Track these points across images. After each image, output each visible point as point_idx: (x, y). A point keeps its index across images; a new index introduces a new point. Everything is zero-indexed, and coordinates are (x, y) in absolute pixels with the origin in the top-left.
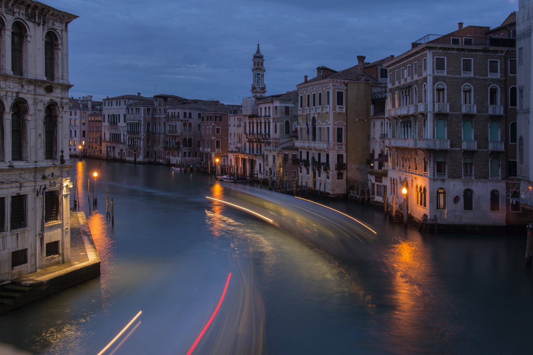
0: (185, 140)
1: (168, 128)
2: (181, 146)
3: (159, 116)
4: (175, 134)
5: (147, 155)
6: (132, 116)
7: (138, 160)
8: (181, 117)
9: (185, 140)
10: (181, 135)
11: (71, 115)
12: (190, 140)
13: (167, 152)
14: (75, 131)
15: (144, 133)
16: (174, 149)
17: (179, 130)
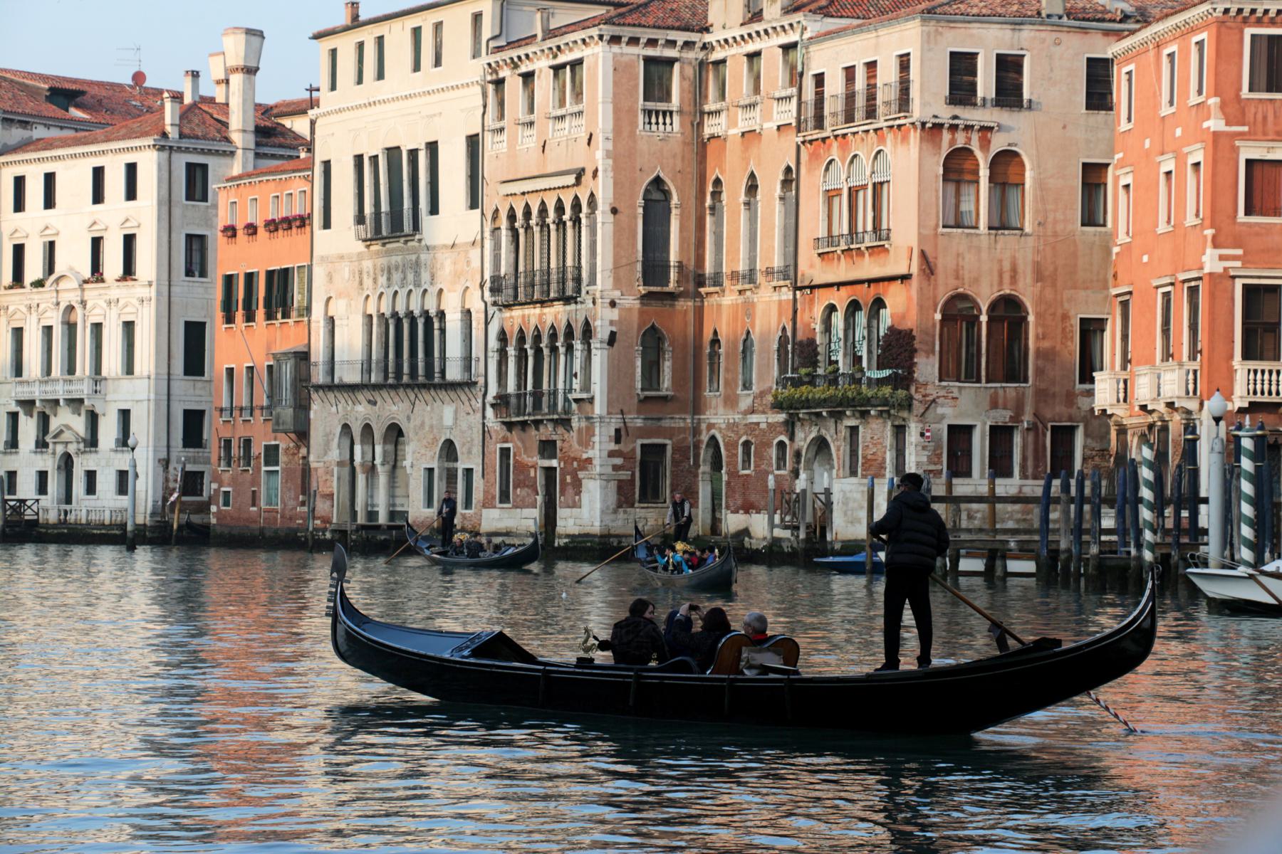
0: (958, 312)
1: (813, 224)
2: (927, 367)
3: (744, 122)
4: (869, 268)
5: (646, 474)
6: (529, 141)
7: (570, 522)
8: (930, 99)
9: (958, 312)
10: (928, 267)
11: (98, 197)
12: (1009, 311)
13: (804, 436)
14: (129, 327)
15: (617, 283)
16: (861, 407)
17: (906, 222)
